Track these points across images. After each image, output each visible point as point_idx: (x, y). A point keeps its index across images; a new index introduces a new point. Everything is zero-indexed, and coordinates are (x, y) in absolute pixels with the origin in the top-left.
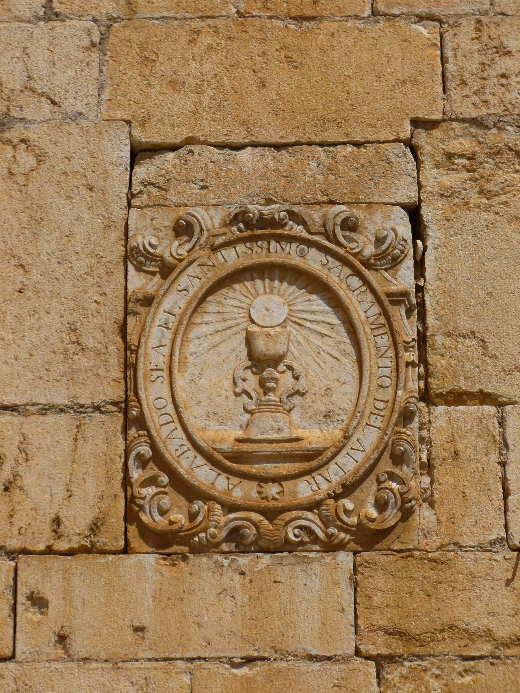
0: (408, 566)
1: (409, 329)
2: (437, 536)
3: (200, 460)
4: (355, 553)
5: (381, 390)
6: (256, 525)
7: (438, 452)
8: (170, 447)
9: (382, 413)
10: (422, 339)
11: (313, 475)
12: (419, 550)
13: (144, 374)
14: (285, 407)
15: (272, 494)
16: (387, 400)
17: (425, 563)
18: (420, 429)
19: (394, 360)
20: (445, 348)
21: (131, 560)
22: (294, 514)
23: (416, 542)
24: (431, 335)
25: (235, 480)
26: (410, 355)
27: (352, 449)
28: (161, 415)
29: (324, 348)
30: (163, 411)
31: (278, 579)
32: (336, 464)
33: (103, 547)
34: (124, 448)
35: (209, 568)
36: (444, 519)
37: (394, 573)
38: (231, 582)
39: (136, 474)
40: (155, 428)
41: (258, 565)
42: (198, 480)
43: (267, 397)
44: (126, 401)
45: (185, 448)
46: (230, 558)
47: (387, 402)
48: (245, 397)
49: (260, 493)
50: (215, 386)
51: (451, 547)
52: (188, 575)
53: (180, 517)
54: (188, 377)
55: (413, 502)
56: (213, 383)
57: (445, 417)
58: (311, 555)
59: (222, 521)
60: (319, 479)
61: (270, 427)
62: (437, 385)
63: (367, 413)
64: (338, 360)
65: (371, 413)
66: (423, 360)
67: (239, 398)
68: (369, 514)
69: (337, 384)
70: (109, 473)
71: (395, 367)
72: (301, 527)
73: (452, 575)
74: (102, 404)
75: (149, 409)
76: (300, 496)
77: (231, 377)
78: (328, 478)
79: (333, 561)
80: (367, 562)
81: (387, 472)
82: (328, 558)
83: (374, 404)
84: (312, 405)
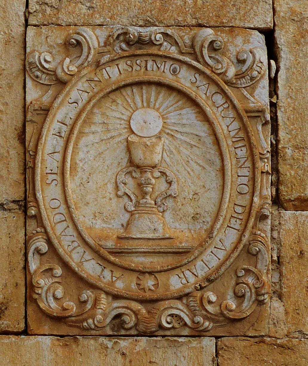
0: (260, 351)
1: (264, 143)
2: (285, 324)
3: (88, 256)
4: (217, 338)
5: (240, 197)
6: (136, 313)
7: (287, 253)
8: (63, 243)
9: (240, 217)
10: (275, 151)
11: (183, 270)
12: (270, 337)
13: (41, 178)
14: (159, 209)
15: (149, 286)
16: (245, 205)
17: (275, 348)
18: (272, 230)
19: (251, 170)
20: (294, 159)
21: (29, 341)
22: (167, 303)
23: (267, 330)
24: (283, 147)
25: (117, 273)
26: (264, 165)
27: (215, 247)
28: (55, 215)
29: (193, 158)
30: (57, 211)
31: (153, 360)
32: (202, 261)
33: (7, 329)
34: (24, 242)
35: (96, 350)
36: (290, 310)
37: (249, 357)
38: (114, 361)
39: (33, 266)
40: (51, 226)
41: (137, 348)
42: (86, 272)
43: (145, 200)
44: (25, 199)
45: (76, 244)
46: (114, 341)
47: (245, 207)
48: (126, 199)
49: (138, 285)
50: (101, 189)
51: (297, 335)
52: (79, 355)
53: (72, 306)
54: (77, 179)
55: (266, 296)
56: (99, 186)
57: (293, 221)
58: (181, 340)
59: (105, 309)
60: (187, 273)
61: (147, 227)
62: (287, 192)
63: (228, 216)
64: (204, 168)
65: (232, 216)
66: (275, 170)
67: (121, 199)
68: (229, 305)
69: (203, 190)
70: (12, 264)
71: (251, 176)
72: (172, 315)
73: (297, 359)
74: (5, 202)
75: (46, 209)
76: (172, 288)
77: (113, 181)
78: (196, 273)
79: (198, 345)
80: (226, 346)
81: (244, 269)
82: (195, 343)
83: (234, 208)
84: (182, 208)
